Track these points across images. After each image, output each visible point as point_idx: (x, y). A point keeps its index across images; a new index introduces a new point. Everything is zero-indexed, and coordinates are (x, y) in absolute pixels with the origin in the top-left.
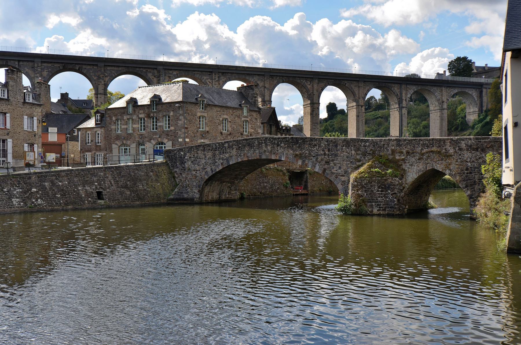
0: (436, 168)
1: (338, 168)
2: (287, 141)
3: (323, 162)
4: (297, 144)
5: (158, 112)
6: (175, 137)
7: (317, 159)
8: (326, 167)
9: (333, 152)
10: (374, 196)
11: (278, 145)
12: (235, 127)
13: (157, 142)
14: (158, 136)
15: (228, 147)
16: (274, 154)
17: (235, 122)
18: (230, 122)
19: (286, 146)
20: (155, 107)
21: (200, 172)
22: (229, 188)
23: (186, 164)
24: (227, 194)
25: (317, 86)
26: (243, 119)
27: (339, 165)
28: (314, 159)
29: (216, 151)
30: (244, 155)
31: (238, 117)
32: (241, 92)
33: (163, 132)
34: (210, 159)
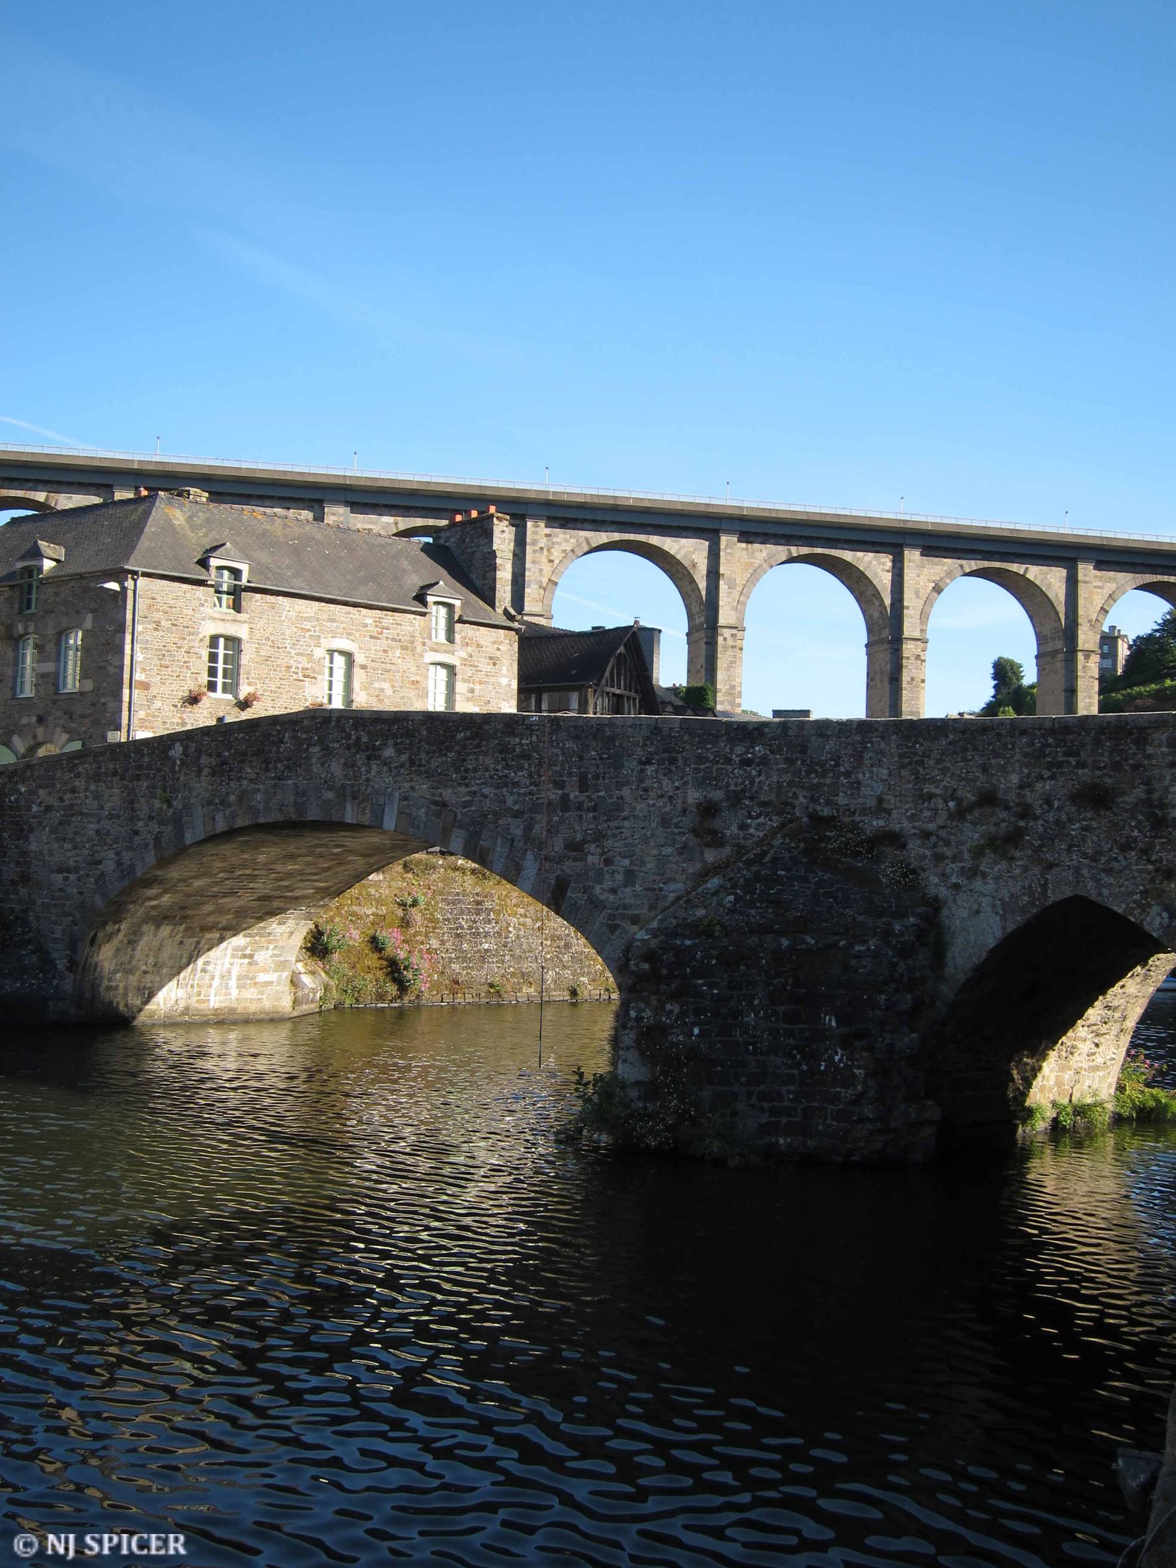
0: (1093, 896)
1: (619, 877)
2: (408, 734)
3: (558, 845)
4: (450, 749)
5: (43, 617)
6: (96, 722)
7: (528, 829)
8: (569, 867)
9: (602, 794)
10: (747, 1044)
11: (373, 755)
12: (389, 692)
13: (32, 742)
14: (34, 719)
15: (183, 763)
16: (354, 798)
18: (363, 667)
19: (404, 757)
20: (34, 596)
21: (79, 880)
22: (244, 956)
23: (32, 837)
24: (233, 983)
25: (918, 576)
27: (626, 862)
28: (518, 831)
29: (138, 778)
30: (241, 798)
31: (404, 648)
32: (447, 547)
33: (55, 702)
34: (118, 816)
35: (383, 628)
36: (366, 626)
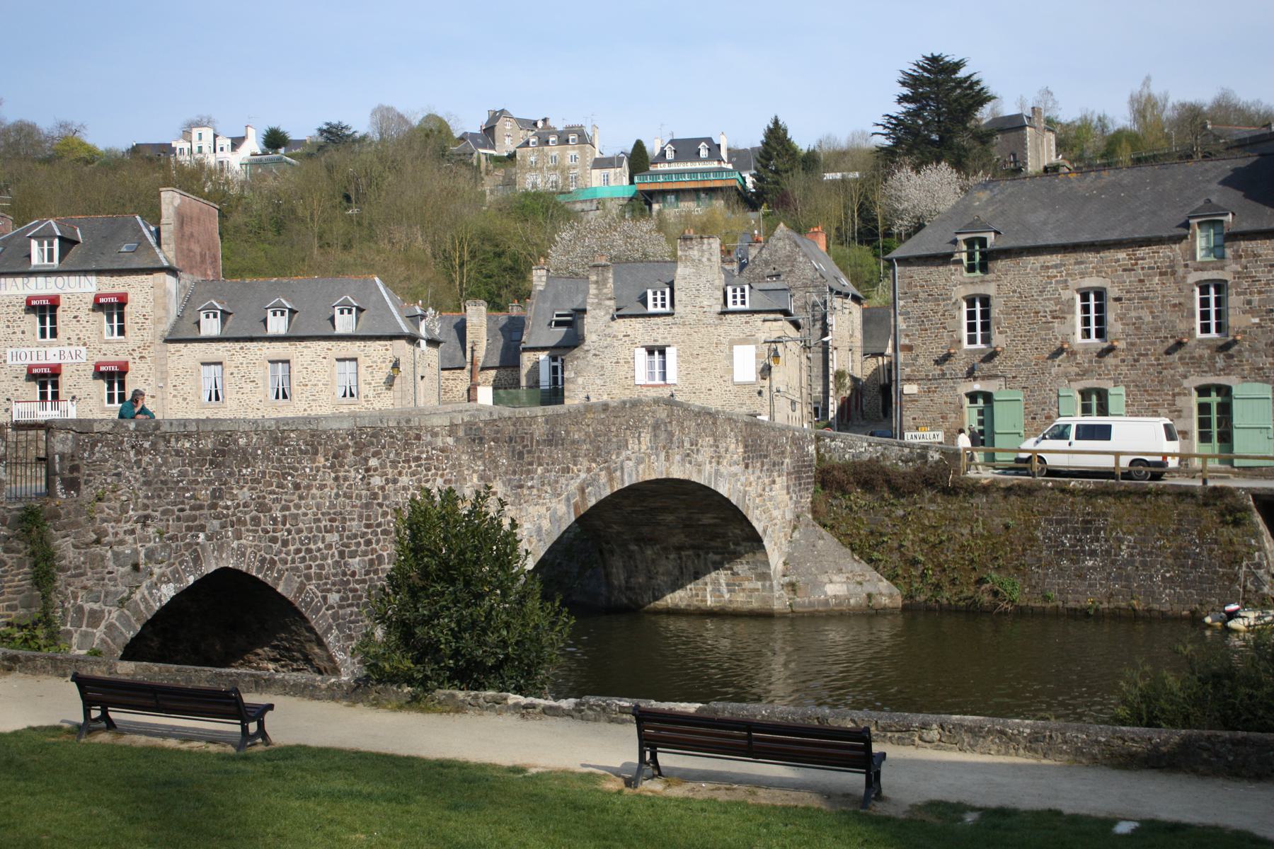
17: (1146, 299)
18: (1118, 299)
26: (1194, 277)
31: (1161, 274)
35: (1137, 259)
36: (1118, 260)
